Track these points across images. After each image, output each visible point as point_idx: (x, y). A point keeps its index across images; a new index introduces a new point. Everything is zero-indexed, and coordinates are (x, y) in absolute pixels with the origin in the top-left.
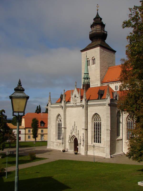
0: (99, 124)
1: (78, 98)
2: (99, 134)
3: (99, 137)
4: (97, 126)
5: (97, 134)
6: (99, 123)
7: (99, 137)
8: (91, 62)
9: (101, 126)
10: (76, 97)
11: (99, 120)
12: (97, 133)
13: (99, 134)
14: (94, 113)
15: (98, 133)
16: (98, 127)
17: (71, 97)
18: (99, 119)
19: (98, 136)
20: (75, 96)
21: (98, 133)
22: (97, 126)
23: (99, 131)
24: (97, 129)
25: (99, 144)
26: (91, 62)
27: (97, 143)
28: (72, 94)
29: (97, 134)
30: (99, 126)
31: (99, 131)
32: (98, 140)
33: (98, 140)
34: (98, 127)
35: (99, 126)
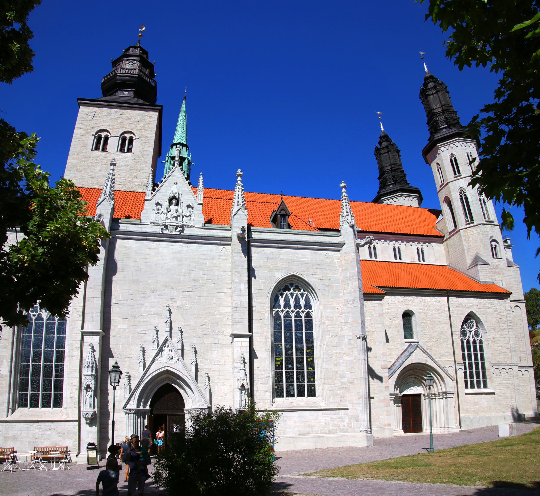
1: (190, 209)
2: (300, 361)
3: (300, 374)
4: (288, 327)
5: (289, 361)
6: (298, 315)
7: (300, 374)
8: (113, 143)
10: (183, 205)
13: (300, 361)
14: (280, 276)
15: (294, 357)
16: (294, 331)
17: (147, 197)
20: (170, 200)
21: (294, 357)
22: (288, 327)
25: (311, 399)
26: (113, 143)
28: (154, 190)
29: (289, 361)
30: (299, 327)
31: (299, 350)
34: (294, 331)
35: (299, 327)
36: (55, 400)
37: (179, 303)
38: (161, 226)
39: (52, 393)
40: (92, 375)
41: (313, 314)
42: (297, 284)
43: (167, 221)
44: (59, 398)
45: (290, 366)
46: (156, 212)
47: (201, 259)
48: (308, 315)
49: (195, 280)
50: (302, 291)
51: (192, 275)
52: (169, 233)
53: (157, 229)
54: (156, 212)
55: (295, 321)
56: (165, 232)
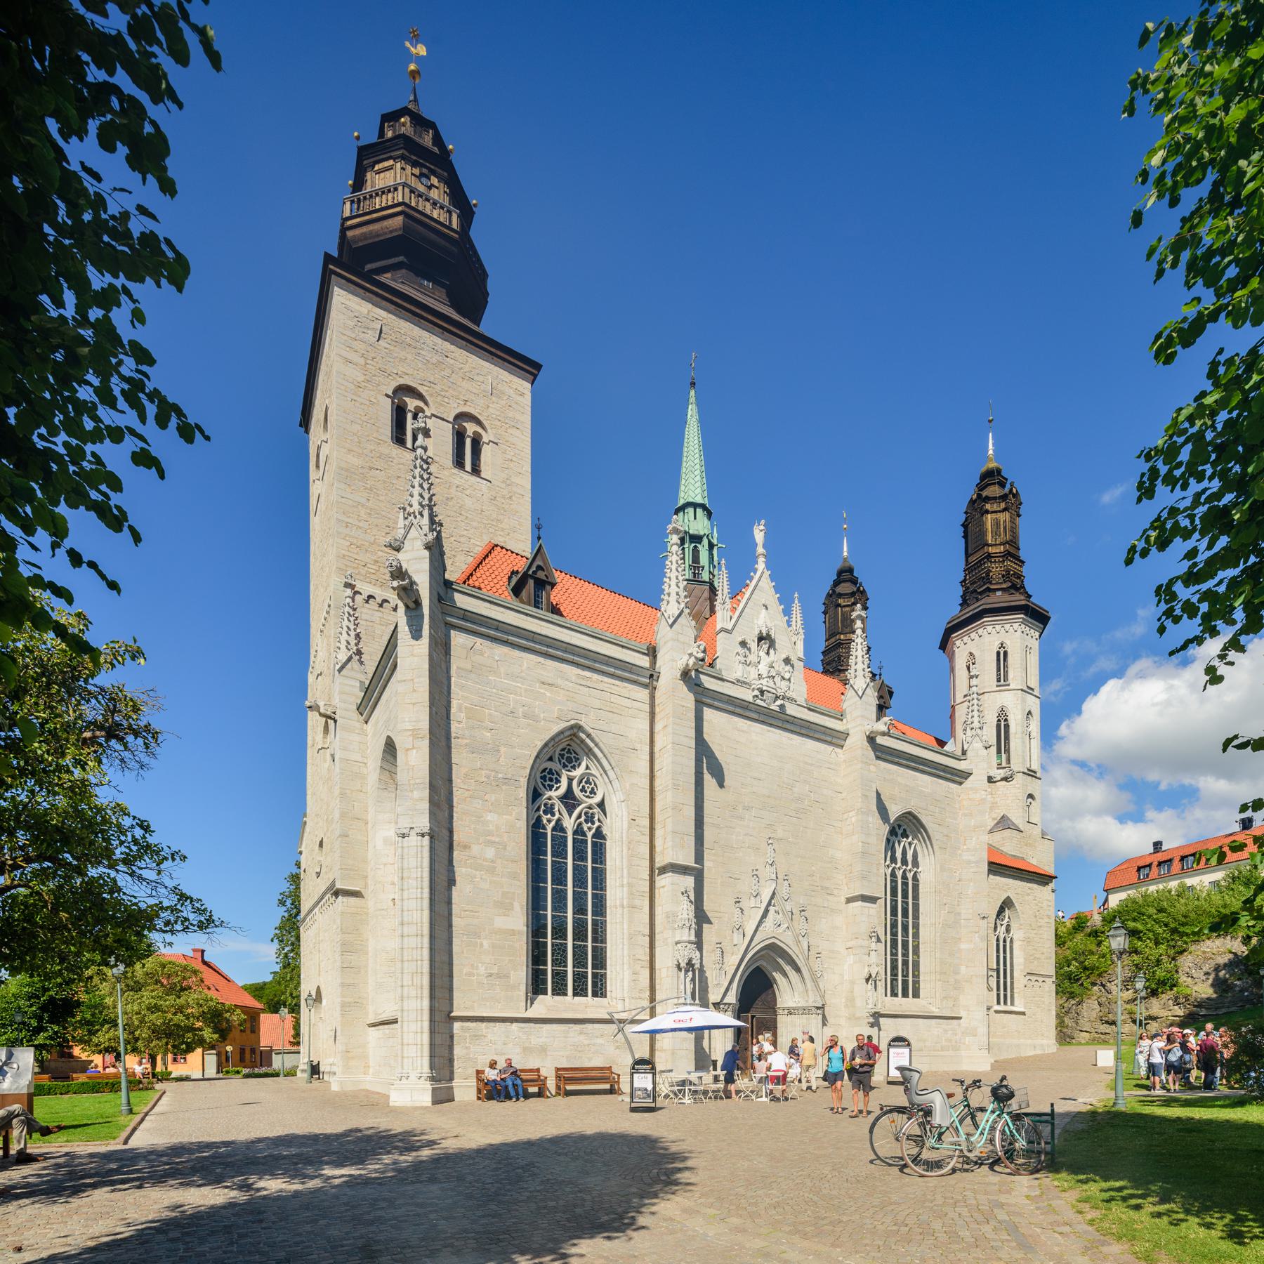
0: (905, 884)
6: (904, 877)
9: (916, 897)
11: (904, 862)
12: (896, 935)
18: (904, 853)
19: (903, 955)
23: (905, 928)
24: (896, 915)
27: (896, 995)
31: (905, 928)
32: (900, 978)
33: (900, 978)
36: (594, 984)
37: (780, 833)
38: (753, 690)
39: (590, 970)
40: (690, 942)
41: (921, 877)
42: (905, 827)
43: (761, 681)
44: (601, 980)
45: (894, 951)
46: (743, 660)
47: (806, 763)
48: (915, 878)
49: (799, 799)
50: (910, 839)
51: (795, 790)
52: (765, 705)
53: (747, 695)
54: (743, 660)
55: (903, 883)
56: (759, 702)
